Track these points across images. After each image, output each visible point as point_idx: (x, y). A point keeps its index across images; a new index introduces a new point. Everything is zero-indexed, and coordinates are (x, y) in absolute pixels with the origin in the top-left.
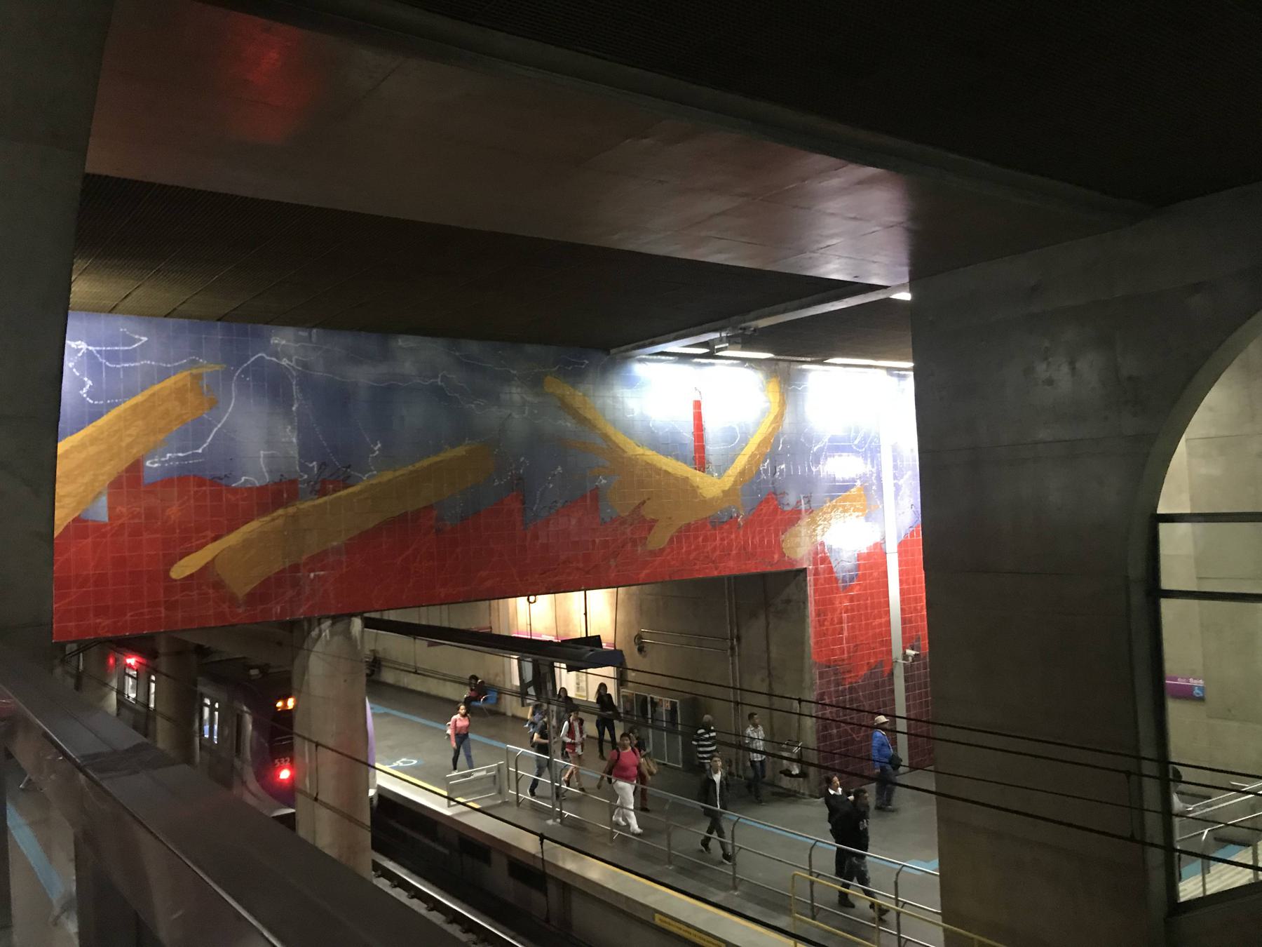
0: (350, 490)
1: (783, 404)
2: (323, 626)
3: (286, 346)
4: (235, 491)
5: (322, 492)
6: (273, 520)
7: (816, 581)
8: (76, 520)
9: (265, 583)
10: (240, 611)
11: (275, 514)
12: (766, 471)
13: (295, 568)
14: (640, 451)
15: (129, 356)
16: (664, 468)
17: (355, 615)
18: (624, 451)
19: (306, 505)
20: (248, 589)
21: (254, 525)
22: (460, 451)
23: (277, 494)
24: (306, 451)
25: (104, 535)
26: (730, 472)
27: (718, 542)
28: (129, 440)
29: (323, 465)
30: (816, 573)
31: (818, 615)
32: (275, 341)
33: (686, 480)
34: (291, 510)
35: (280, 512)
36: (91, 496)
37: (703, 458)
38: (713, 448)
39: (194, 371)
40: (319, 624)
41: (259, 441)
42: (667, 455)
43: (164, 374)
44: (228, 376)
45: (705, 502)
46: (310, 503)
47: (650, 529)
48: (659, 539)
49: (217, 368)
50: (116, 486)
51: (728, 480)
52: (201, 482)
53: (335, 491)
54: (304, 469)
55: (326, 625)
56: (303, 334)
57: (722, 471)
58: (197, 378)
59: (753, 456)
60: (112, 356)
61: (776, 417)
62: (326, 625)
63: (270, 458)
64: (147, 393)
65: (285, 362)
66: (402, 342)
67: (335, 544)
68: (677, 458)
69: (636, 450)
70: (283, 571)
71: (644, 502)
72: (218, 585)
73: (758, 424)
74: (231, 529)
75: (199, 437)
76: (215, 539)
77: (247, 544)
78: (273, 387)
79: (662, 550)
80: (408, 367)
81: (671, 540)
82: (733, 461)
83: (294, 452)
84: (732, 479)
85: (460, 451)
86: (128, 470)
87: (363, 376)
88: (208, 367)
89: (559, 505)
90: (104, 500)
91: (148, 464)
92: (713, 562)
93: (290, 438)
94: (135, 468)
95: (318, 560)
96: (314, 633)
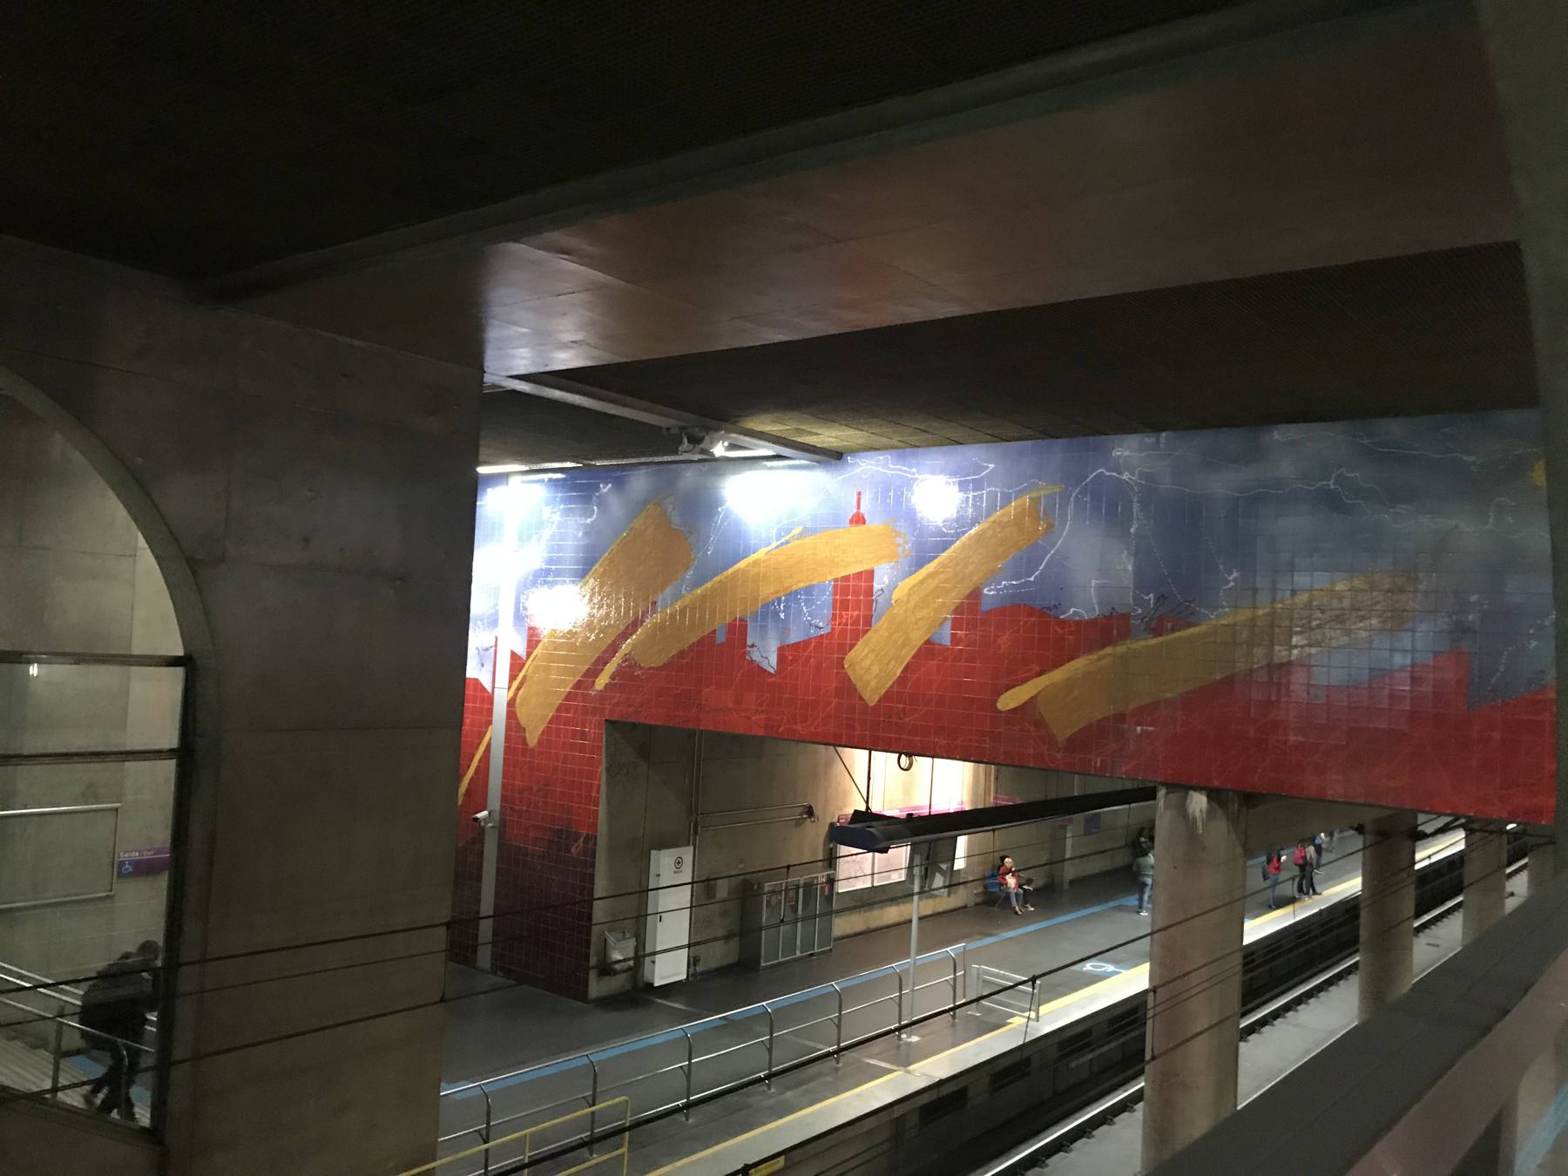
0: (1192, 630)
3: (1130, 456)
4: (1063, 623)
5: (1157, 631)
6: (1100, 659)
8: (928, 642)
9: (1087, 730)
10: (1059, 756)
11: (1102, 653)
13: (1120, 718)
17: (1196, 789)
19: (1138, 645)
20: (1068, 733)
21: (1077, 665)
23: (1107, 629)
24: (1143, 581)
25: (945, 659)
29: (1161, 598)
32: (1117, 453)
34: (1120, 649)
35: (1109, 650)
39: (1034, 495)
41: (1095, 568)
43: (1007, 499)
44: (1065, 497)
46: (1143, 643)
49: (1056, 489)
50: (958, 610)
52: (1031, 611)
53: (1173, 630)
54: (1138, 601)
56: (1149, 440)
63: (1100, 588)
64: (991, 519)
66: (1279, 434)
67: (1169, 695)
70: (1106, 718)
72: (1040, 724)
74: (1057, 664)
75: (1032, 564)
76: (1040, 674)
77: (1070, 684)
78: (1108, 505)
80: (1285, 467)
83: (1128, 582)
86: (969, 597)
87: (1221, 484)
88: (1046, 489)
91: (985, 591)
93: (1125, 565)
94: (975, 595)
95: (1146, 713)
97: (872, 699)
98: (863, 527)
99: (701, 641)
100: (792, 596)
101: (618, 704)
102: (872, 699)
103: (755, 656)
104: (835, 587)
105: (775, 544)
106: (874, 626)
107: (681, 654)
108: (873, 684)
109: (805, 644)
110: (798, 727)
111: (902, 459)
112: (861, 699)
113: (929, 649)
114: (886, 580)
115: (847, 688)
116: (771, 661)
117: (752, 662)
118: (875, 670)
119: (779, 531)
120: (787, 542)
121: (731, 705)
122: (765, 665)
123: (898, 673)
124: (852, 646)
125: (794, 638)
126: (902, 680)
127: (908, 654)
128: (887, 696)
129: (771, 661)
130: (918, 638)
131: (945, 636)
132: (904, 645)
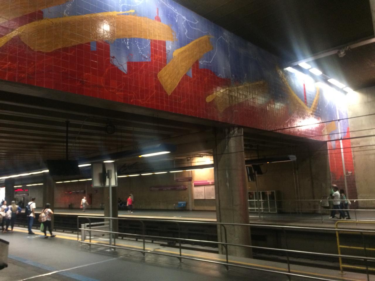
2: (235, 130)
4: (218, 78)
8: (186, 75)
15: (195, 26)
28: (195, 53)
36: (188, 69)
38: (308, 99)
40: (234, 129)
43: (202, 35)
50: (193, 66)
55: (236, 129)
58: (209, 38)
60: (191, 24)
62: (236, 129)
65: (226, 41)
69: (294, 95)
83: (230, 70)
90: (191, 70)
91: (200, 62)
94: (197, 62)
96: (231, 133)
97: (169, 93)
98: (160, 23)
99: (80, 46)
100: (132, 40)
101: (10, 69)
102: (169, 93)
103: (115, 63)
104: (151, 43)
105: (121, 12)
106: (167, 65)
107: (65, 49)
108: (169, 86)
109: (141, 63)
110: (140, 100)
112: (165, 92)
113: (186, 77)
114: (170, 47)
115: (159, 87)
116: (124, 68)
117: (113, 65)
118: (169, 81)
119: (124, 7)
120: (128, 14)
121: (103, 85)
122: (121, 68)
123: (177, 84)
124: (160, 70)
125: (135, 59)
126: (179, 87)
127: (180, 77)
128: (174, 92)
129: (124, 68)
130: (182, 73)
131: (190, 75)
132: (178, 74)
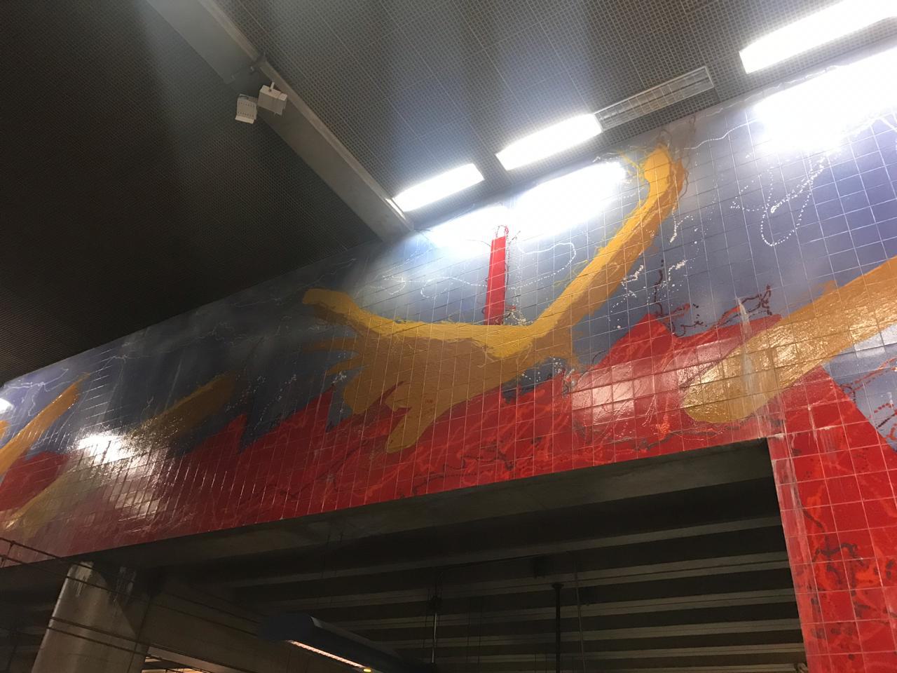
1: (678, 176)
7: (804, 469)
12: (632, 286)
14: (401, 327)
16: (432, 337)
18: (378, 335)
22: (209, 387)
26: (550, 310)
27: (518, 420)
30: (803, 445)
31: (826, 548)
33: (466, 343)
37: (502, 305)
38: (519, 288)
42: (439, 321)
45: (497, 364)
47: (397, 421)
48: (405, 436)
51: (545, 324)
57: (533, 313)
59: (606, 271)
61: (664, 198)
68: (455, 319)
71: (394, 388)
73: (615, 226)
79: (409, 451)
81: (427, 434)
82: (560, 291)
84: (557, 317)
85: (209, 387)
89: (282, 417)
92: (503, 457)
111: (28, 380)
